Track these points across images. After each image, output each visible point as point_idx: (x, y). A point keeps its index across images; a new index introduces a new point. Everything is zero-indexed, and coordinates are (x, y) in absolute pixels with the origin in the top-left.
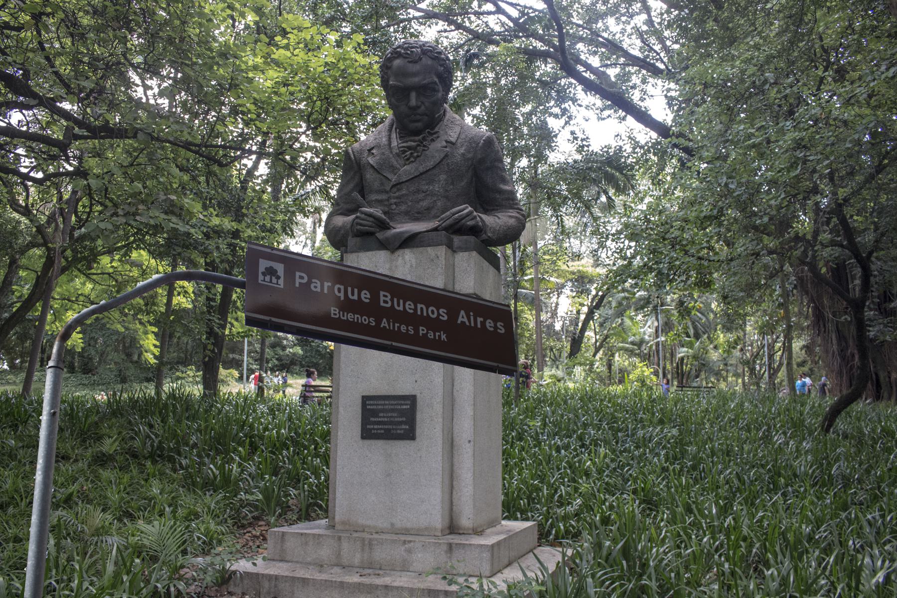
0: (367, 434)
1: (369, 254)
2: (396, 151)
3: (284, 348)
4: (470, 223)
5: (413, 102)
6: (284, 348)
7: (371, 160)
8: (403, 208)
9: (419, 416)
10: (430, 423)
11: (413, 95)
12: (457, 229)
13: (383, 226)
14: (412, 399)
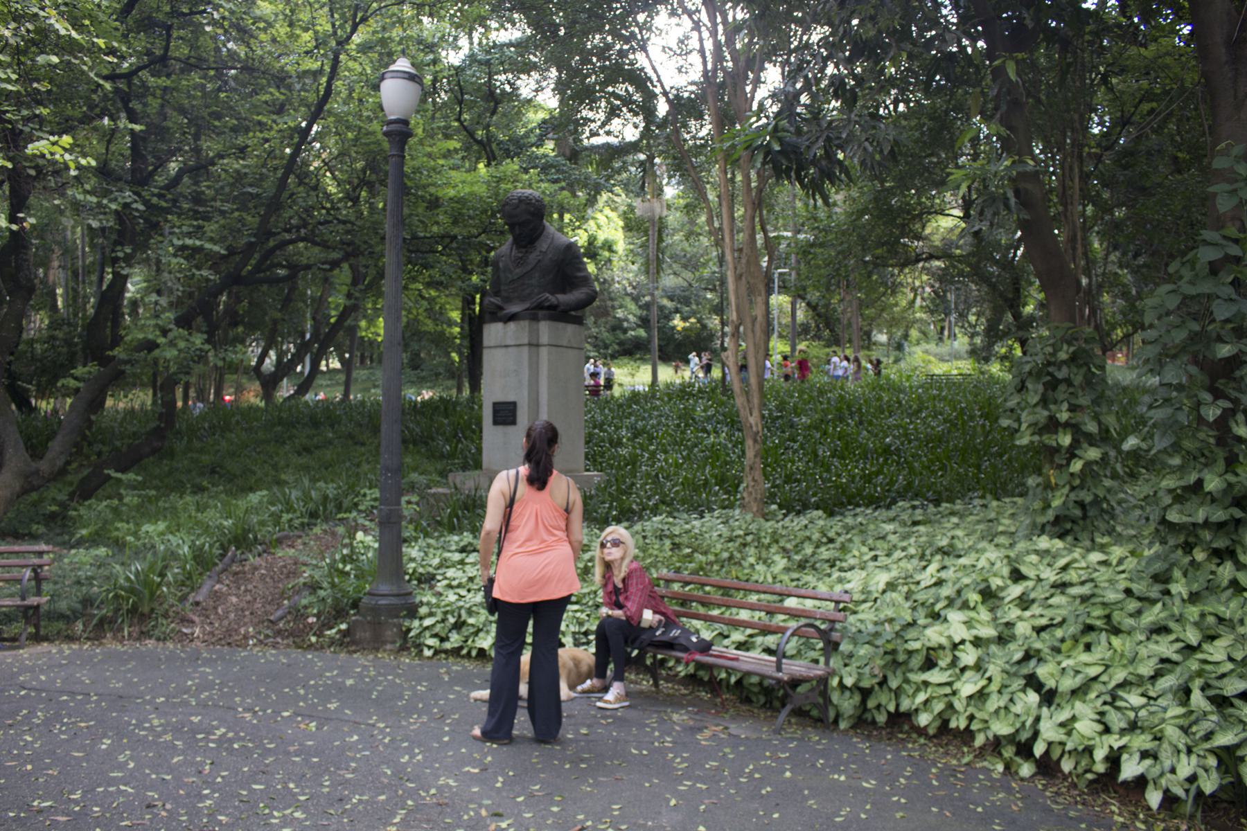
0: (496, 422)
3: (625, 331)
6: (625, 331)
13: (501, 308)
14: (514, 404)
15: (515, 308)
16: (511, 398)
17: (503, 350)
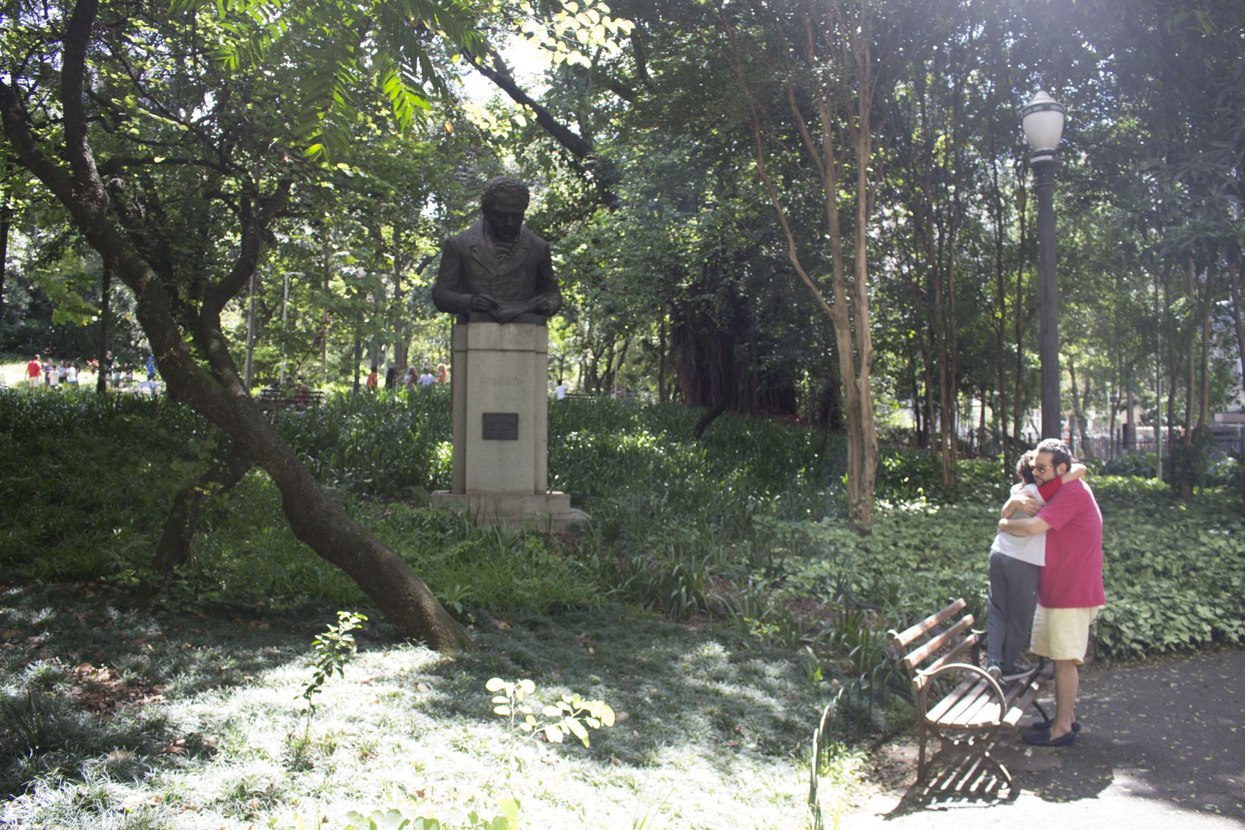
8: (500, 292)
9: (520, 426)
14: (515, 417)
15: (507, 309)
16: (510, 409)
17: (499, 355)
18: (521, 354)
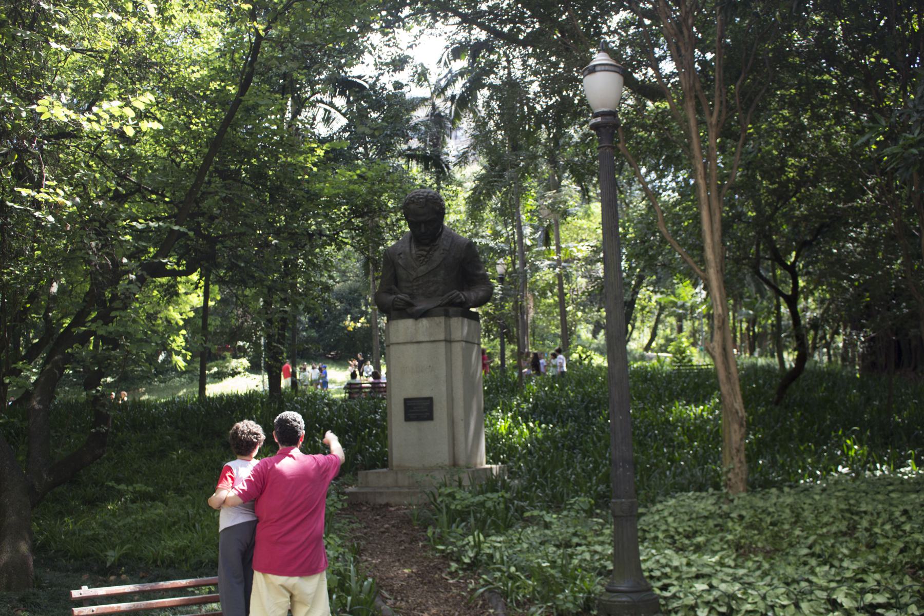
0: (408, 418)
1: (403, 321)
2: (414, 256)
4: (458, 301)
5: (423, 230)
7: (400, 262)
8: (420, 291)
9: (435, 408)
10: (440, 410)
11: (423, 226)
12: (451, 303)
13: (411, 305)
14: (430, 400)
15: (421, 306)
16: (426, 394)
17: (416, 346)
18: (435, 345)
